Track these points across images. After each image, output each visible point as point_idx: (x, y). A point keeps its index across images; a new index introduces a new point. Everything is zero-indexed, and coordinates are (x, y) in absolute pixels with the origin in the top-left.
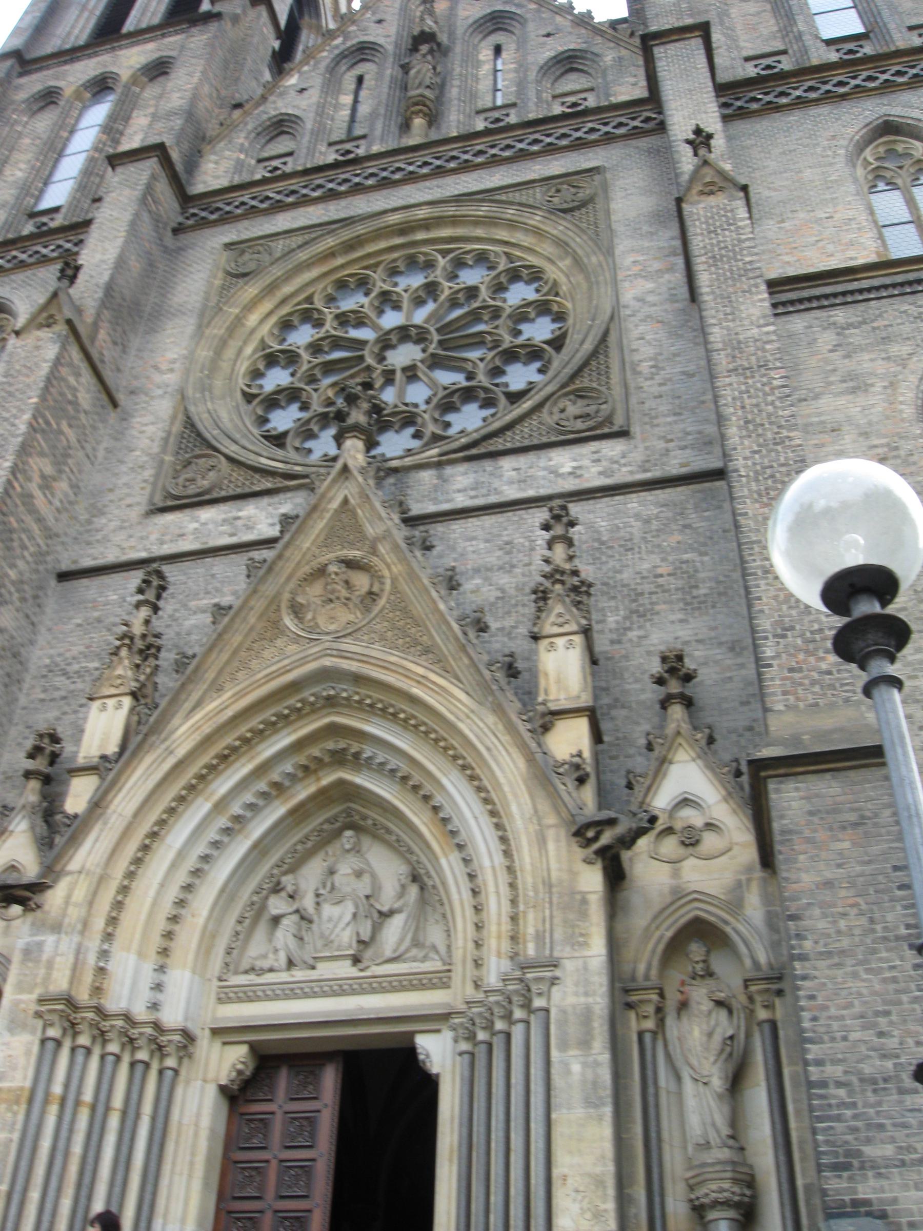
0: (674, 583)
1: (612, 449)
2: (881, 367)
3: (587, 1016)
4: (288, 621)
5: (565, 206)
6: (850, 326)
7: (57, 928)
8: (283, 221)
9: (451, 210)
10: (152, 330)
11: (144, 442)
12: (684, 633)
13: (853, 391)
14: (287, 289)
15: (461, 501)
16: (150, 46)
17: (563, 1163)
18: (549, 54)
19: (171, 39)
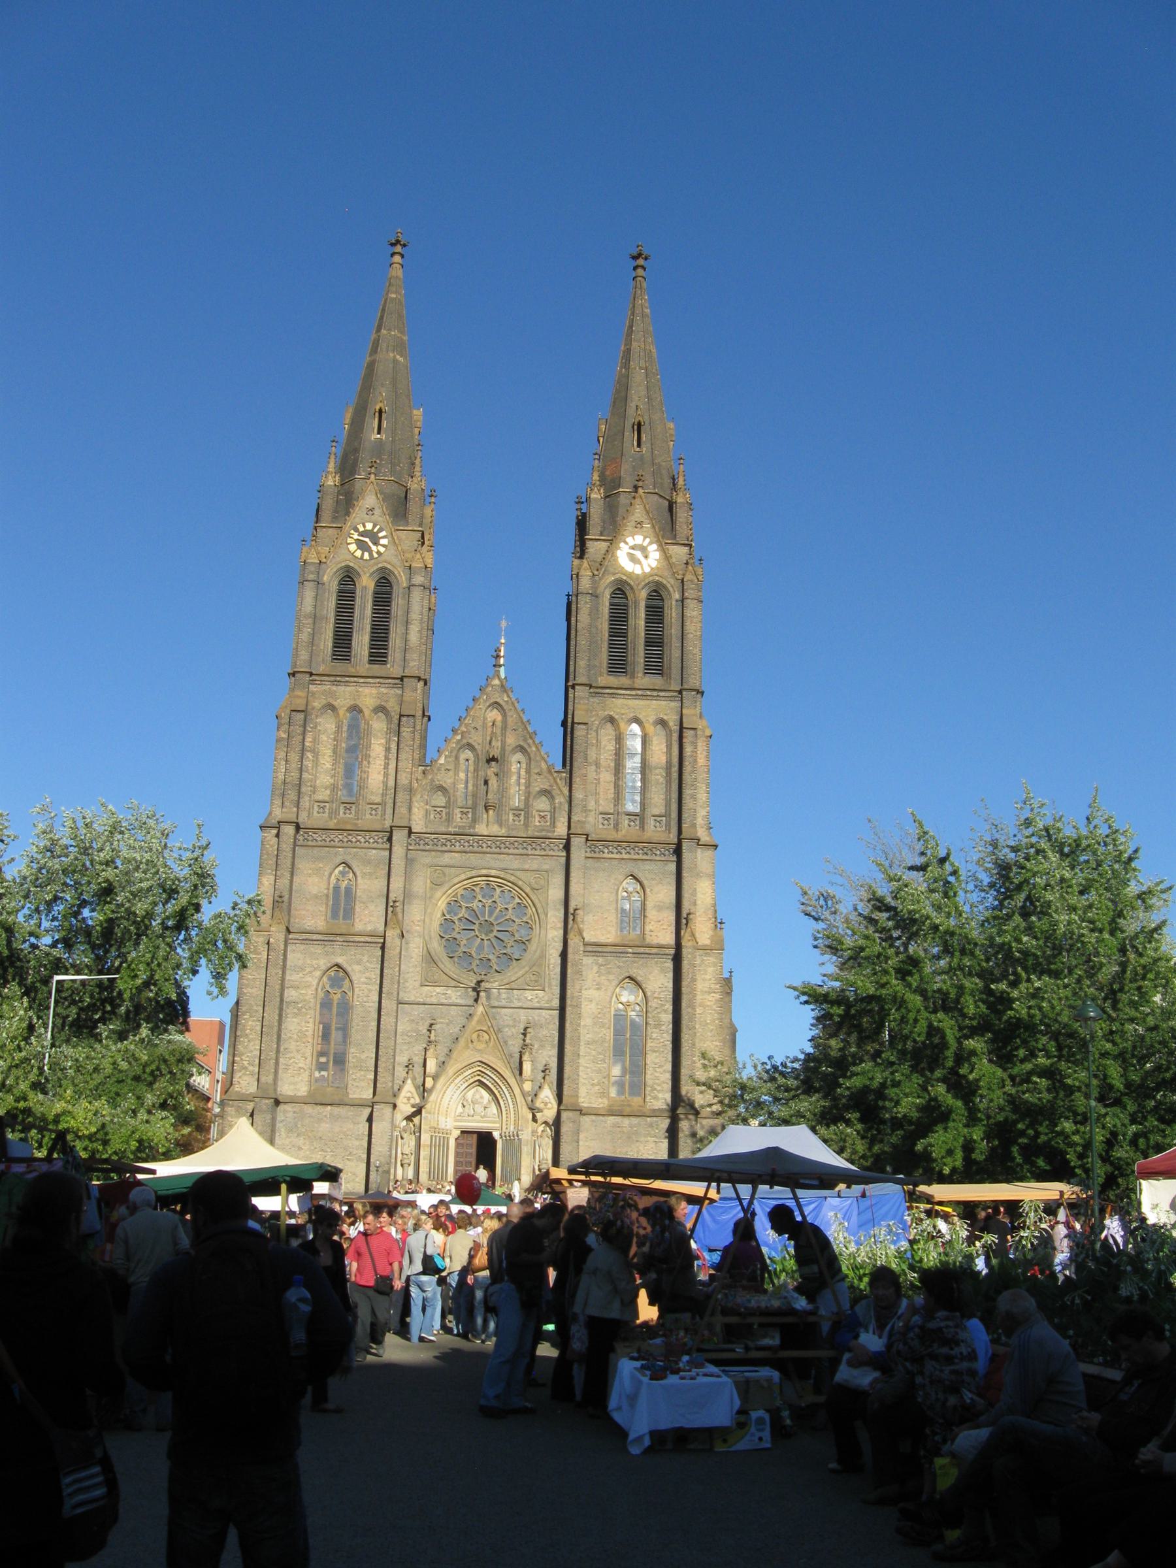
0: (550, 1039)
1: (541, 994)
2: (606, 983)
3: (527, 1141)
4: (470, 1045)
5: (536, 886)
6: (602, 965)
7: (430, 1113)
8: (447, 859)
9: (502, 874)
10: (409, 903)
11: (414, 955)
12: (550, 1053)
13: (598, 989)
14: (450, 891)
15: (504, 1003)
16: (374, 691)
17: (523, 1163)
18: (537, 789)
19: (384, 690)
